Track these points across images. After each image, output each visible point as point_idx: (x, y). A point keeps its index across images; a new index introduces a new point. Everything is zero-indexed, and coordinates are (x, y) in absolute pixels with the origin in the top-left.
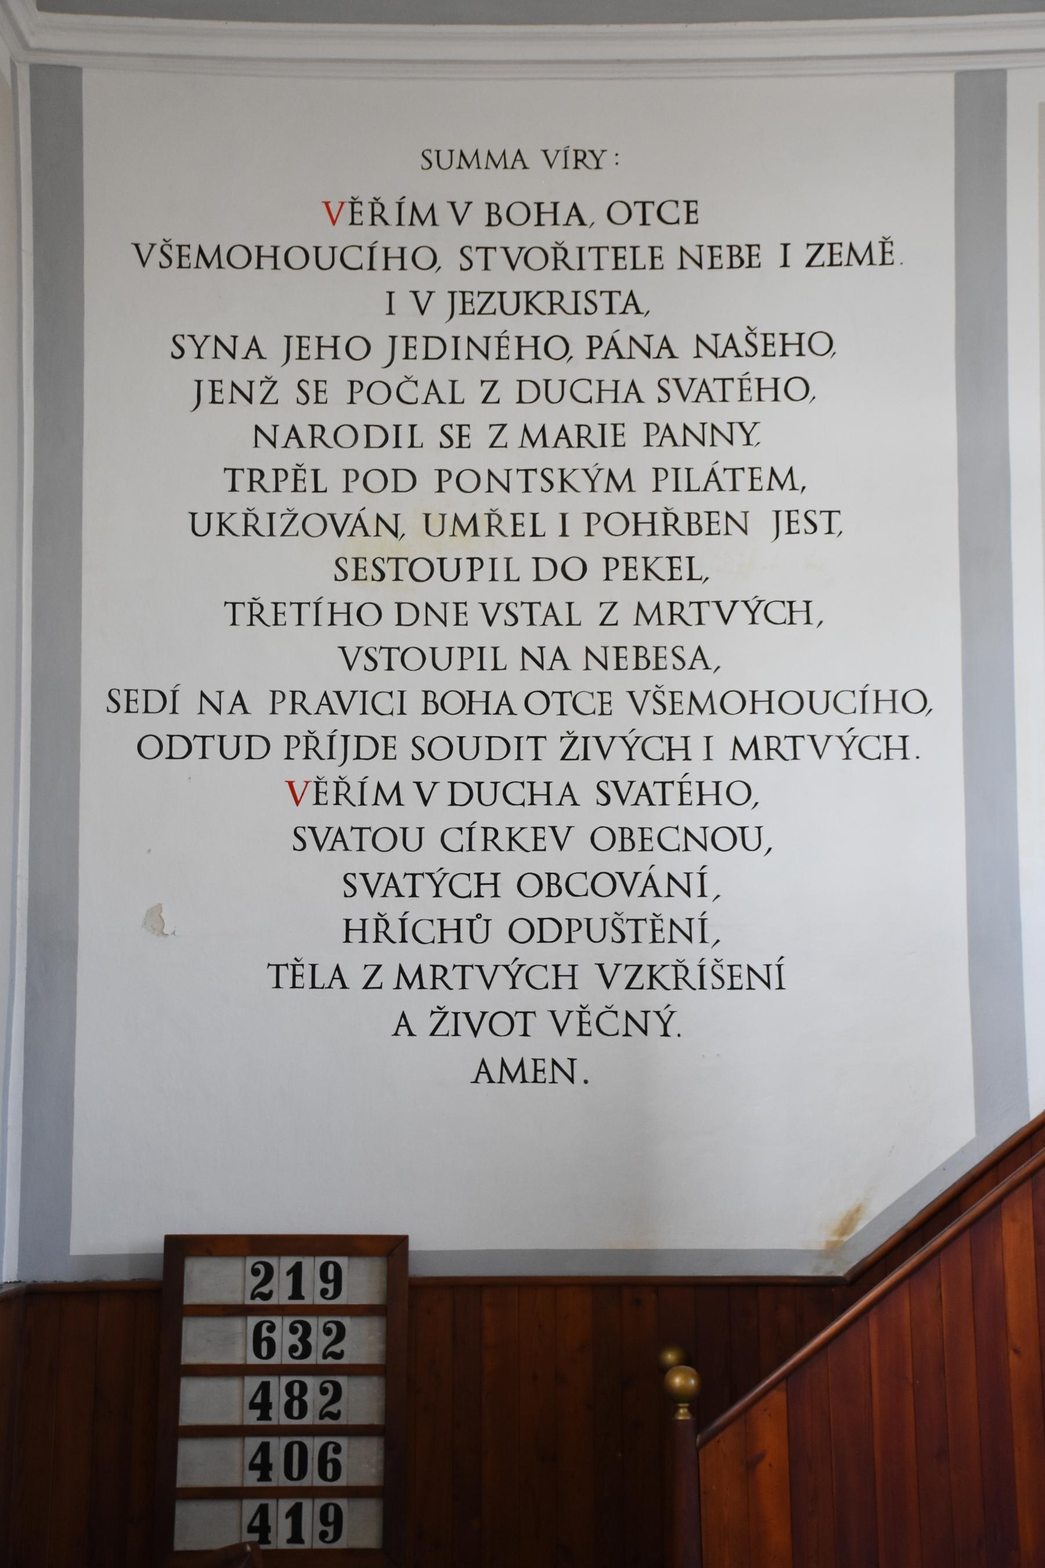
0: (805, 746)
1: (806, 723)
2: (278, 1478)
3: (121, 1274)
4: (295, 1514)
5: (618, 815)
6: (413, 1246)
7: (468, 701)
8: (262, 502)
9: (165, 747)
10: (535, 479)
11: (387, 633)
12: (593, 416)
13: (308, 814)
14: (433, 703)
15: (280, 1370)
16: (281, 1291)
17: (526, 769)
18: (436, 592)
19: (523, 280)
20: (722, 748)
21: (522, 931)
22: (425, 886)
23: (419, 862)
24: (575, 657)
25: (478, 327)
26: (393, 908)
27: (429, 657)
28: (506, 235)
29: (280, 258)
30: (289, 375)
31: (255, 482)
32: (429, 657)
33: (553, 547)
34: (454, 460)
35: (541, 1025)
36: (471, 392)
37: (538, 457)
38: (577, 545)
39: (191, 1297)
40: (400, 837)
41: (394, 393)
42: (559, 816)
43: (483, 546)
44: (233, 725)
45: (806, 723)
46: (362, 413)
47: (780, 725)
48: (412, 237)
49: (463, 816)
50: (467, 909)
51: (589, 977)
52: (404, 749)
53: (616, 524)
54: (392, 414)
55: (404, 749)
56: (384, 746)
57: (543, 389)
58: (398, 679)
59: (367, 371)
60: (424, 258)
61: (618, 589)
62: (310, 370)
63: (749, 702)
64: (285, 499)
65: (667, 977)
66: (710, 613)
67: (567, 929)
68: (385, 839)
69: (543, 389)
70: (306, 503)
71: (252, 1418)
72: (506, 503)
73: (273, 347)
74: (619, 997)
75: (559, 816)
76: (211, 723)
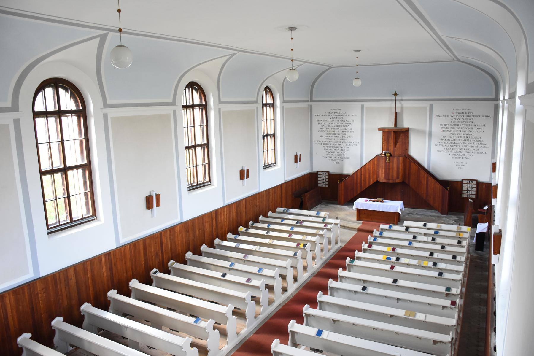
5: (341, 149)
11: (329, 138)
12: (340, 125)
14: (331, 142)
16: (323, 174)
18: (331, 135)
24: (339, 139)
27: (331, 139)
28: (335, 114)
29: (323, 115)
32: (331, 139)
33: (338, 133)
34: (332, 127)
35: (337, 160)
36: (333, 123)
37: (337, 127)
41: (329, 123)
43: (334, 133)
44: (321, 143)
46: (327, 125)
47: (351, 144)
52: (329, 144)
54: (329, 125)
56: (329, 144)
57: (337, 123)
59: (328, 122)
62: (324, 122)
63: (349, 142)
67: (338, 155)
69: (337, 123)
70: (324, 130)
73: (323, 121)
76: (319, 143)
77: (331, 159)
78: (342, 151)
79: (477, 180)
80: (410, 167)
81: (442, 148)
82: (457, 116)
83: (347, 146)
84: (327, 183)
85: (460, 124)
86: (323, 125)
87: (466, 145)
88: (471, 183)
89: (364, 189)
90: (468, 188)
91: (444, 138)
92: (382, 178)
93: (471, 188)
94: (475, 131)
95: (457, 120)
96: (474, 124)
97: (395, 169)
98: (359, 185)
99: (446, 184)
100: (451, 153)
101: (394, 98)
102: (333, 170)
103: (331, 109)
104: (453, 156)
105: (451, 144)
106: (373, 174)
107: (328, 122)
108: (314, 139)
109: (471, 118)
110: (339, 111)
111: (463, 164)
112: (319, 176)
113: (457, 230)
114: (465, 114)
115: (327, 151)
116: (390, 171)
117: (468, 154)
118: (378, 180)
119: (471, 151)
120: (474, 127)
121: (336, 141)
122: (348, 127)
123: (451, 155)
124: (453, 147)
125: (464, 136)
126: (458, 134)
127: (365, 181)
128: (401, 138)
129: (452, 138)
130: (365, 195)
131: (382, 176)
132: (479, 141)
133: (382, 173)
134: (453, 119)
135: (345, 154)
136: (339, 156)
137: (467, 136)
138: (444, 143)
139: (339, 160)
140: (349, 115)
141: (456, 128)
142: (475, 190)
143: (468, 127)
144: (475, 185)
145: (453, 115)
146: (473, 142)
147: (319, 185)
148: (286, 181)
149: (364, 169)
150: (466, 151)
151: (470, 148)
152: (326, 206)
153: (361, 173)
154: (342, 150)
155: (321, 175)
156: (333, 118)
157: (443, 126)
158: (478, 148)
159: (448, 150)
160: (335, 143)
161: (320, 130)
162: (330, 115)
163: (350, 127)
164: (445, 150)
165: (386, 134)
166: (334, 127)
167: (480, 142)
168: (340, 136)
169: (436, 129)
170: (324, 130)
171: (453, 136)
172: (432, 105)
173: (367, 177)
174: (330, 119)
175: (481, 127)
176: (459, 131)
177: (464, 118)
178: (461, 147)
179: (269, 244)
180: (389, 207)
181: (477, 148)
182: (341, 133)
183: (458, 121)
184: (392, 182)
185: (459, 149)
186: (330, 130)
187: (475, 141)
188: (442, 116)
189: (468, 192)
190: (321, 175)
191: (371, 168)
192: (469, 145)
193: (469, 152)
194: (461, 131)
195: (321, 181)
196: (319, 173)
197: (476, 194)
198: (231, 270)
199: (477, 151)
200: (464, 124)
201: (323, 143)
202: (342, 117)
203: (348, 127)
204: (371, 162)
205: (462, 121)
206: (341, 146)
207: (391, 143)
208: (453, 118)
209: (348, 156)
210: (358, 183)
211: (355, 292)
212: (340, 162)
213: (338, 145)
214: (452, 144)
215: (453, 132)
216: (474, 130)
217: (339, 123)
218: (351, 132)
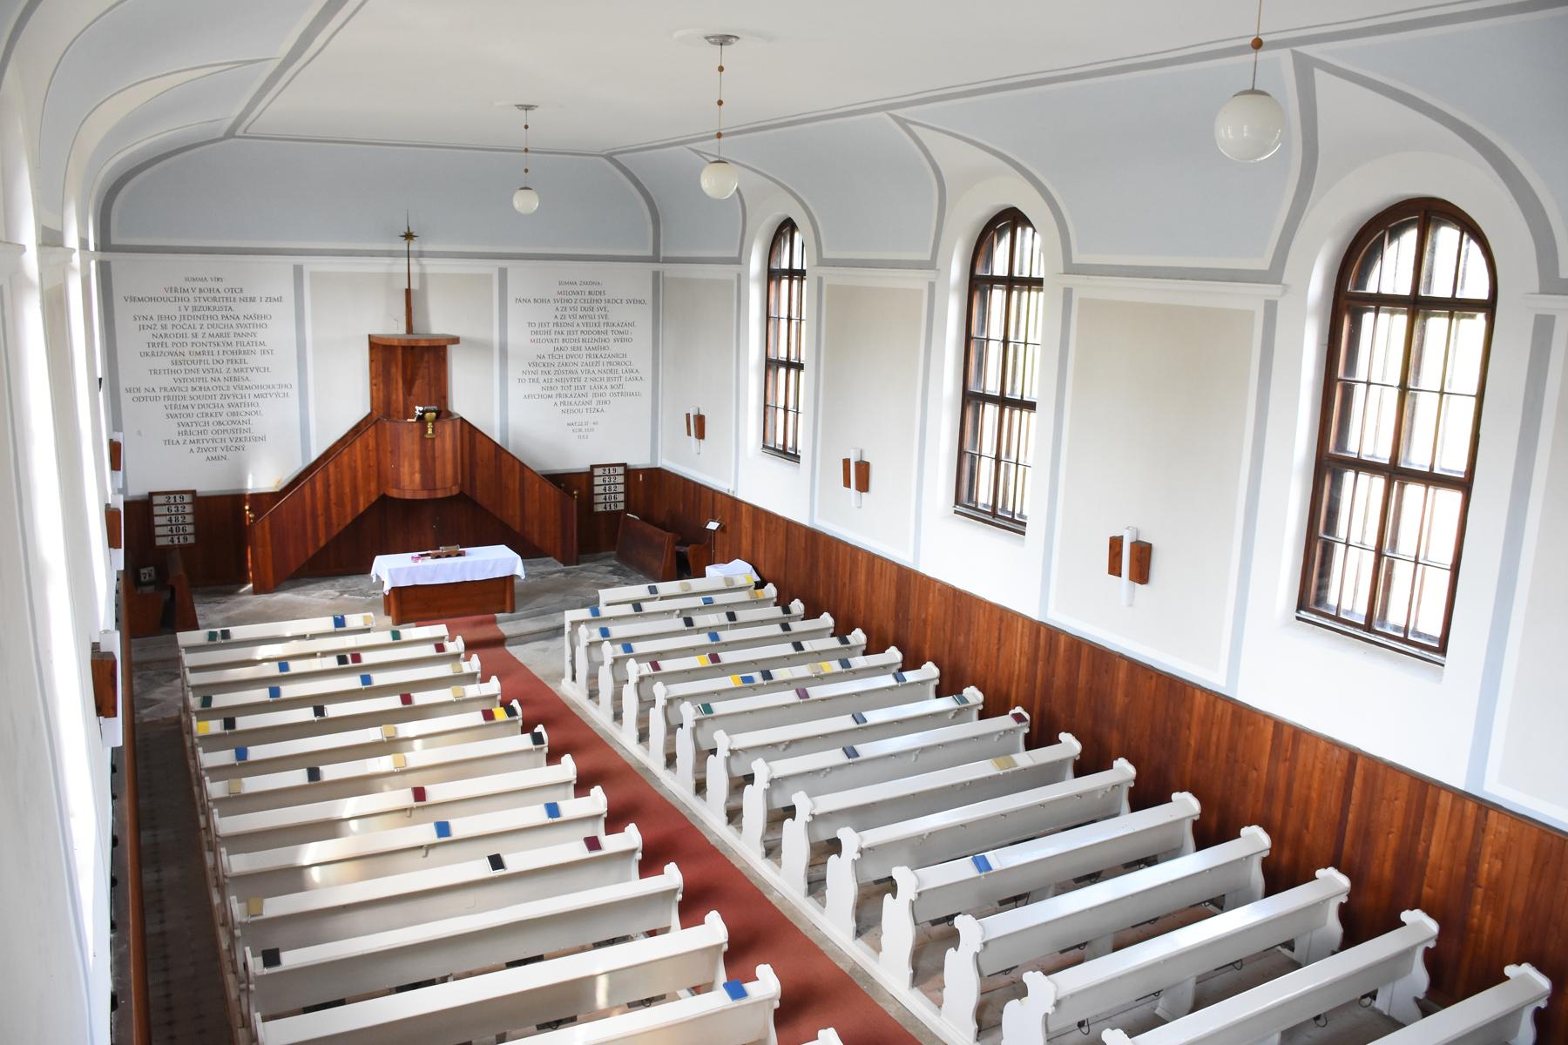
1: (268, 391)
2: (175, 532)
3: (139, 499)
4: (179, 538)
5: (232, 410)
7: (200, 388)
8: (155, 350)
9: (139, 399)
10: (212, 345)
12: (223, 331)
13: (169, 411)
14: (194, 389)
16: (172, 501)
17: (213, 401)
18: (192, 367)
19: (207, 304)
21: (214, 432)
22: (194, 424)
25: (199, 313)
26: (188, 429)
27: (192, 380)
29: (156, 300)
30: (159, 324)
31: (153, 345)
32: (192, 380)
33: (216, 357)
34: (195, 340)
37: (212, 339)
38: (221, 357)
39: (155, 503)
40: (188, 415)
41: (182, 327)
42: (220, 410)
43: (203, 358)
44: (153, 394)
45: (268, 391)
46: (175, 331)
47: (263, 391)
50: (203, 429)
51: (228, 441)
53: (229, 353)
54: (182, 331)
55: (188, 398)
56: (184, 398)
57: (213, 326)
58: (186, 385)
59: (176, 322)
61: (230, 365)
62: (164, 322)
63: (257, 387)
64: (160, 349)
65: (243, 439)
66: (249, 370)
67: (223, 432)
69: (213, 326)
70: (164, 349)
73: (155, 317)
74: (234, 444)
75: (220, 410)
76: (148, 394)
77: (194, 447)
78: (235, 418)
81: (536, 389)
82: (568, 301)
83: (253, 400)
84: (190, 529)
85: (576, 321)
87: (593, 376)
89: (341, 528)
90: (607, 487)
92: (409, 482)
94: (612, 341)
95: (568, 312)
97: (449, 455)
98: (321, 520)
100: (558, 400)
102: (209, 480)
103: (187, 279)
109: (603, 305)
110: (215, 285)
111: (591, 426)
112: (157, 510)
113: (726, 587)
114: (587, 297)
115: (179, 420)
117: (599, 398)
118: (394, 493)
120: (609, 329)
121: (211, 384)
122: (253, 339)
125: (588, 352)
127: (340, 503)
128: (425, 365)
129: (560, 361)
131: (412, 481)
133: (412, 474)
135: (245, 427)
136: (226, 436)
137: (596, 352)
139: (228, 449)
140: (253, 300)
141: (569, 333)
142: (622, 490)
144: (622, 477)
145: (559, 297)
147: (160, 542)
149: (336, 467)
152: (223, 606)
153: (328, 480)
154: (233, 414)
155: (165, 505)
156: (195, 308)
157: (536, 329)
160: (209, 393)
162: (182, 300)
163: (259, 339)
164: (544, 392)
165: (380, 355)
166: (200, 339)
167: (624, 368)
168: (224, 367)
169: (518, 336)
170: (164, 349)
174: (184, 312)
175: (626, 328)
177: (586, 305)
178: (583, 383)
179: (388, 742)
180: (490, 567)
181: (620, 382)
183: (572, 313)
186: (186, 350)
188: (532, 301)
190: (165, 505)
192: (601, 375)
193: (601, 395)
195: (167, 525)
196: (157, 500)
197: (154, 529)
198: (431, 852)
199: (620, 391)
200: (588, 321)
201: (163, 394)
203: (253, 339)
205: (582, 313)
206: (232, 400)
207: (397, 383)
208: (559, 305)
209: (257, 430)
210: (320, 512)
211: (833, 768)
212: (229, 455)
213: (218, 397)
214: (560, 376)
215: (560, 344)
216: (611, 336)
217: (218, 326)
218: (263, 352)
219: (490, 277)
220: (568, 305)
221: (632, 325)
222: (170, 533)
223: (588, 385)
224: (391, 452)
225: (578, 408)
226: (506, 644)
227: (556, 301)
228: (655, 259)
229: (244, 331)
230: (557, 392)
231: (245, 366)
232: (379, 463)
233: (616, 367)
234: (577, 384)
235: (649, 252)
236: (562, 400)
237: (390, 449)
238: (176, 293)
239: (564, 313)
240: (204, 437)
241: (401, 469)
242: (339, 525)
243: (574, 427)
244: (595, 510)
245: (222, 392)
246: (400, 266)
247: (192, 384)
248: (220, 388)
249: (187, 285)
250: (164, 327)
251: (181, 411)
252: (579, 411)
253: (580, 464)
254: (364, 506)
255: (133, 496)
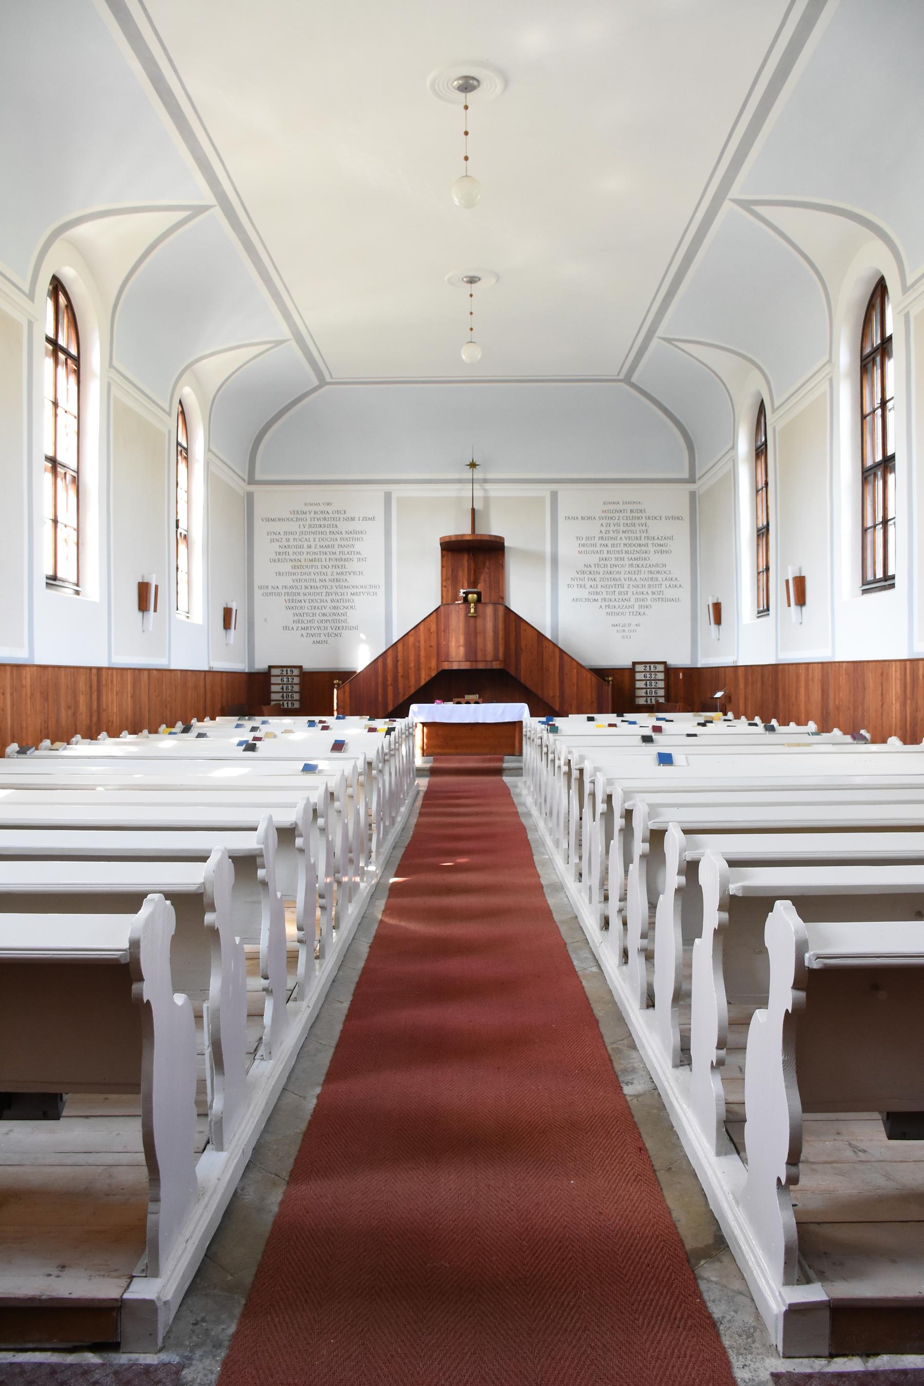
0: (361, 594)
1: (361, 590)
2: (285, 698)
4: (288, 703)
5: (333, 604)
6: (303, 667)
7: (311, 587)
8: (280, 557)
11: (299, 577)
12: (330, 543)
13: (288, 604)
14: (306, 587)
15: (285, 684)
16: (285, 673)
19: (320, 523)
20: (349, 594)
21: (319, 621)
22: (305, 615)
23: (304, 611)
24: (327, 580)
25: (313, 530)
26: (300, 618)
27: (305, 580)
28: (317, 516)
29: (283, 520)
30: (284, 538)
32: (305, 580)
33: (324, 563)
34: (309, 550)
36: (312, 540)
37: (322, 550)
38: (328, 563)
39: (272, 674)
40: (301, 608)
42: (325, 604)
43: (313, 563)
44: (276, 591)
45: (361, 590)
46: (295, 543)
48: (303, 516)
49: (311, 604)
50: (311, 618)
51: (329, 628)
52: (302, 594)
53: (334, 560)
54: (300, 543)
55: (302, 594)
56: (299, 594)
57: (323, 539)
59: (296, 537)
60: (305, 519)
62: (287, 537)
63: (353, 587)
65: (341, 628)
66: (348, 573)
67: (326, 621)
68: (299, 608)
69: (323, 539)
70: (287, 557)
71: (281, 690)
72: (317, 557)
73: (282, 533)
75: (325, 604)
76: (273, 591)
77: (304, 632)
79: (664, 663)
80: (518, 635)
81: (584, 593)
82: (611, 518)
83: (350, 597)
85: (619, 536)
86: (284, 543)
87: (635, 583)
88: (652, 669)
89: (406, 697)
90: (648, 682)
91: (586, 569)
93: (653, 682)
94: (652, 552)
95: (612, 528)
96: (652, 533)
98: (390, 689)
99: (601, 673)
100: (604, 604)
101: (467, 474)
103: (306, 504)
104: (609, 610)
105: (603, 583)
106: (428, 657)
107: (296, 537)
108: (257, 582)
109: (643, 521)
110: (326, 508)
112: (273, 680)
116: (480, 639)
117: (641, 603)
118: (446, 666)
119: (647, 596)
120: (650, 542)
121: (319, 584)
123: (604, 607)
124: (607, 590)
125: (631, 562)
126: (617, 559)
127: (406, 677)
128: (487, 570)
129: (605, 569)
130: (426, 695)
132: (663, 572)
133: (459, 647)
134: (605, 525)
135: (343, 618)
136: (328, 625)
138: (586, 579)
139: (329, 635)
140: (353, 519)
141: (613, 545)
142: (663, 686)
143: (639, 542)
145: (603, 515)
146: (651, 576)
148: (211, 670)
150: (637, 596)
151: (645, 590)
156: (310, 526)
158: (662, 590)
159: (596, 597)
161: (274, 556)
162: (302, 519)
163: (355, 550)
164: (590, 597)
166: (313, 550)
167: (664, 576)
168: (329, 571)
169: (567, 548)
171: (606, 562)
172: (557, 492)
173: (412, 665)
174: (302, 529)
175: (665, 541)
176: (618, 552)
177: (629, 522)
178: (625, 589)
182: (332, 563)
183: (615, 528)
184: (485, 668)
185: (620, 593)
186: (302, 558)
187: (655, 572)
189: (648, 692)
191: (422, 642)
192: (642, 583)
193: (643, 600)
194: (624, 552)
196: (274, 672)
199: (660, 596)
200: (630, 535)
202: (335, 523)
204: (421, 627)
205: (625, 529)
206: (333, 597)
208: (604, 522)
209: (352, 622)
210: (389, 683)
212: (330, 640)
214: (606, 583)
215: (605, 555)
216: (651, 549)
218: (359, 560)
219: (543, 498)
220: (611, 522)
221: (671, 538)
222: (281, 699)
223: (630, 591)
224: (444, 631)
225: (622, 610)
226: (504, 774)
227: (601, 518)
228: (692, 480)
229: (345, 543)
230: (602, 597)
231: (345, 570)
232: (438, 644)
233: (657, 576)
234: (621, 590)
235: (686, 475)
236: (607, 603)
237: (443, 628)
238: (298, 515)
239: (608, 528)
240: (311, 625)
241: (450, 644)
242: (404, 695)
243: (617, 628)
244: (637, 703)
245: (327, 590)
246: (466, 491)
247: (305, 584)
248: (326, 587)
249: (306, 509)
250: (288, 540)
251: (296, 604)
252: (622, 613)
253: (623, 661)
254: (425, 680)
255: (259, 669)
